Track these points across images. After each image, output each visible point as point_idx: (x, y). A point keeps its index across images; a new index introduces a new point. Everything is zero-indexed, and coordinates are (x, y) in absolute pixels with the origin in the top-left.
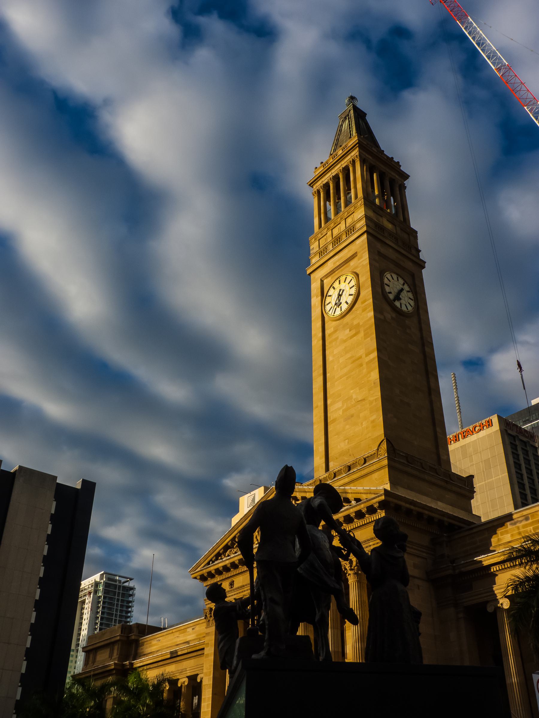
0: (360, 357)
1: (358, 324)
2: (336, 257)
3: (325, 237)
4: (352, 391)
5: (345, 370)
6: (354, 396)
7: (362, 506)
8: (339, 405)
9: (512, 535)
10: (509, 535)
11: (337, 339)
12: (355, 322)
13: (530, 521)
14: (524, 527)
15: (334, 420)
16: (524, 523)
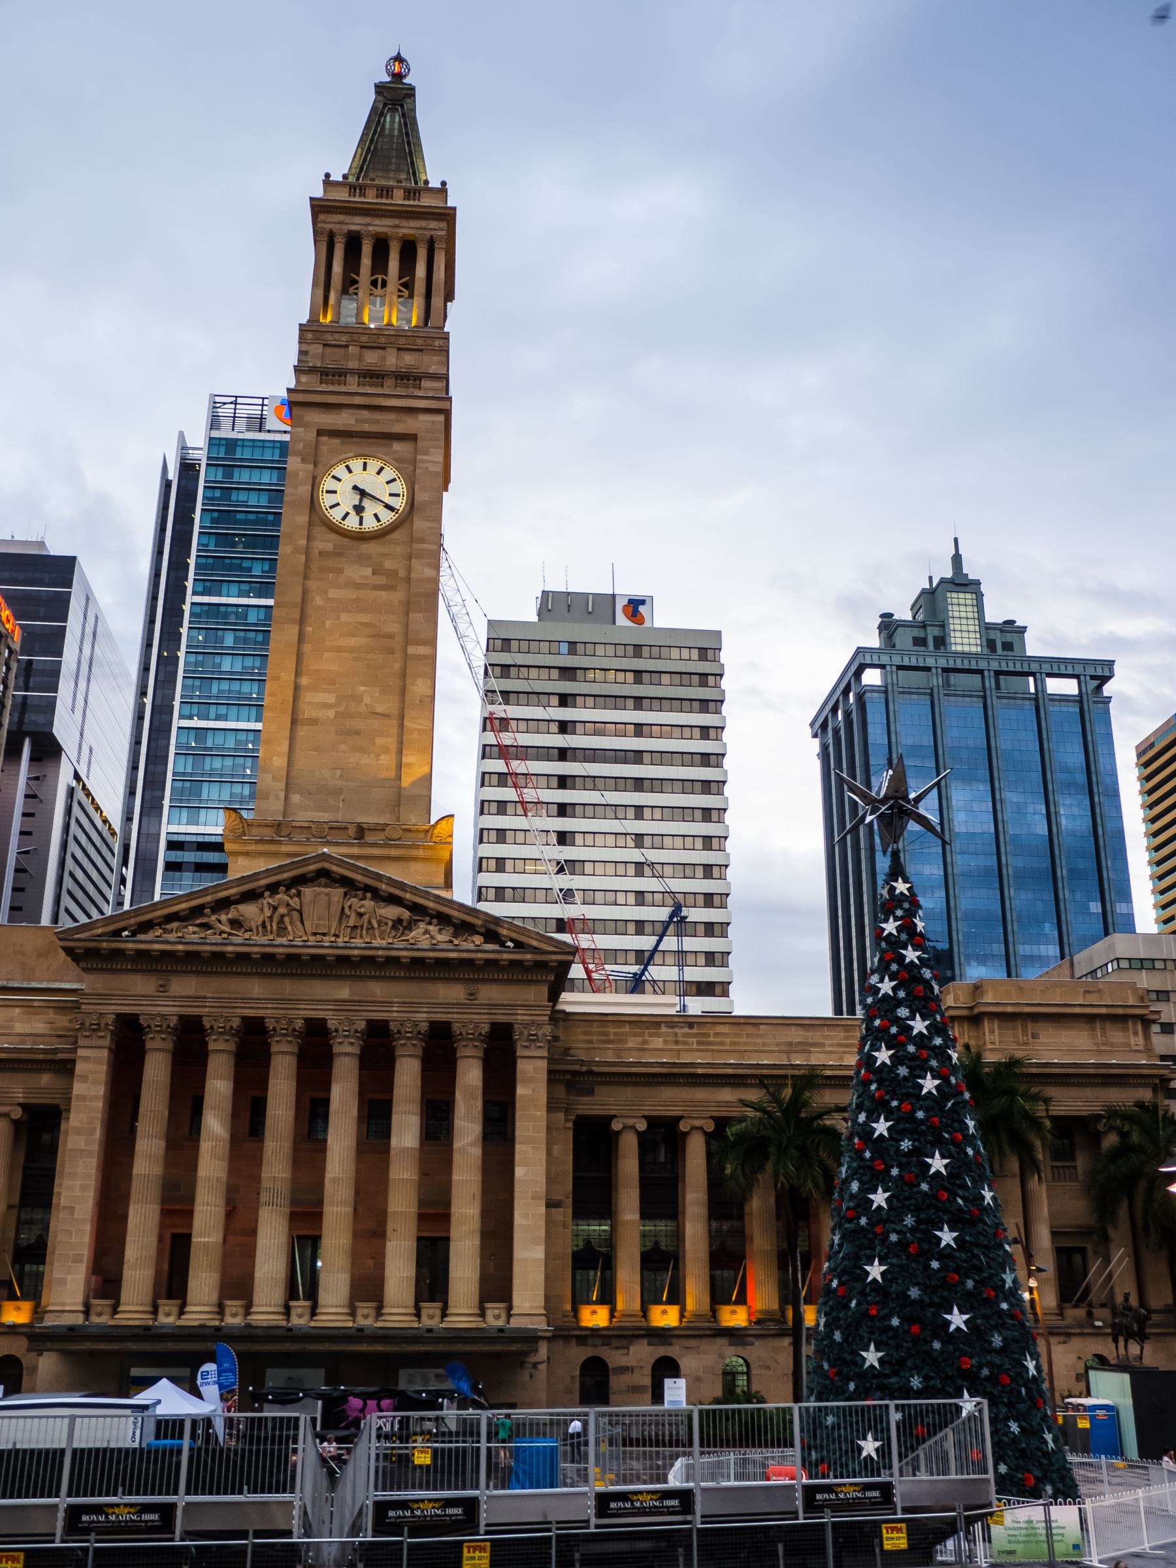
0: (391, 636)
1: (396, 572)
2: (365, 414)
3: (342, 351)
4: (363, 688)
5: (353, 642)
6: (367, 699)
7: (529, 957)
8: (330, 698)
9: (665, 1042)
10: (661, 1040)
11: (341, 571)
12: (388, 565)
13: (694, 1031)
14: (684, 1035)
15: (313, 722)
16: (686, 1030)
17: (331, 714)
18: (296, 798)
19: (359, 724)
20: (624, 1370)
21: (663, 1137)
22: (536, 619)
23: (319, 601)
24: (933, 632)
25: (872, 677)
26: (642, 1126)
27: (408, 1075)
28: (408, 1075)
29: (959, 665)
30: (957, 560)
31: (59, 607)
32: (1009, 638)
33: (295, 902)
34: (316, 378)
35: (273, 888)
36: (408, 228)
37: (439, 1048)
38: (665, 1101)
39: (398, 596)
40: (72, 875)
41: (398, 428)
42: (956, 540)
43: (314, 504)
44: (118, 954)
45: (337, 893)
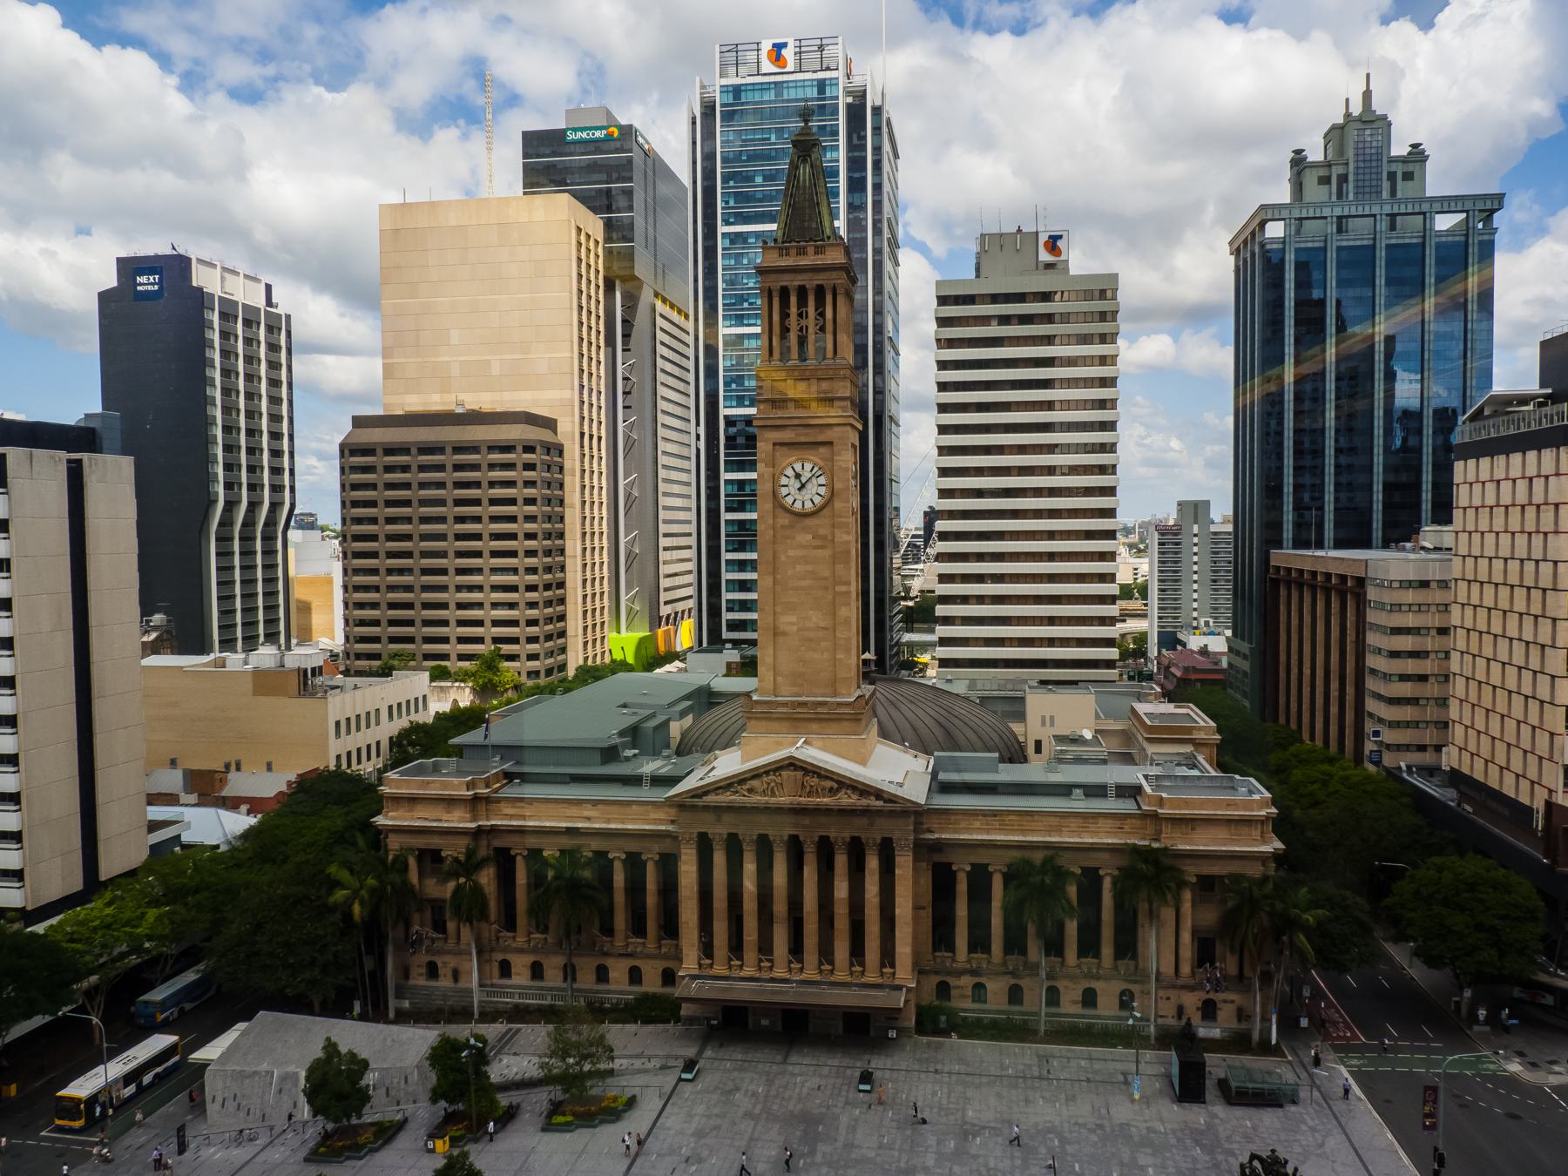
1: (824, 538)
2: (802, 431)
8: (793, 619)
12: (822, 532)
15: (785, 634)
17: (795, 628)
18: (780, 679)
19: (811, 634)
20: (958, 987)
21: (980, 878)
22: (973, 276)
23: (783, 558)
24: (1336, 171)
25: (1275, 230)
26: (968, 868)
27: (841, 861)
28: (841, 861)
29: (1353, 212)
30: (1367, 95)
31: (623, 170)
32: (1410, 168)
33: (778, 780)
34: (768, 406)
35: (767, 773)
36: (820, 279)
37: (857, 852)
38: (981, 858)
39: (826, 553)
40: (663, 371)
41: (821, 438)
42: (1368, 76)
43: (775, 494)
44: (694, 807)
45: (800, 774)
